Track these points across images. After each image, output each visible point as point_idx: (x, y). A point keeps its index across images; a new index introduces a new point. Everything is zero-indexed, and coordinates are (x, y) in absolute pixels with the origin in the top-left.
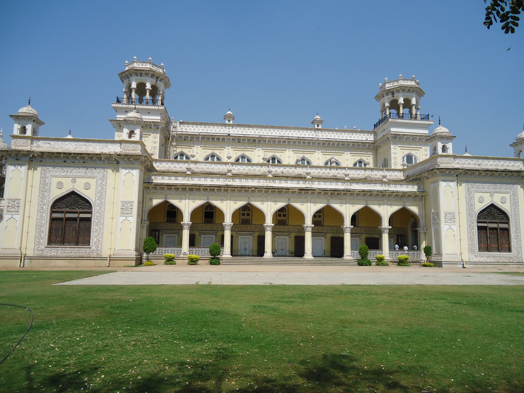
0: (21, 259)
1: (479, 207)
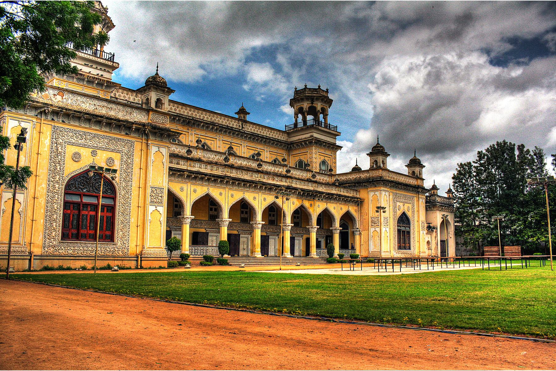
0: (30, 260)
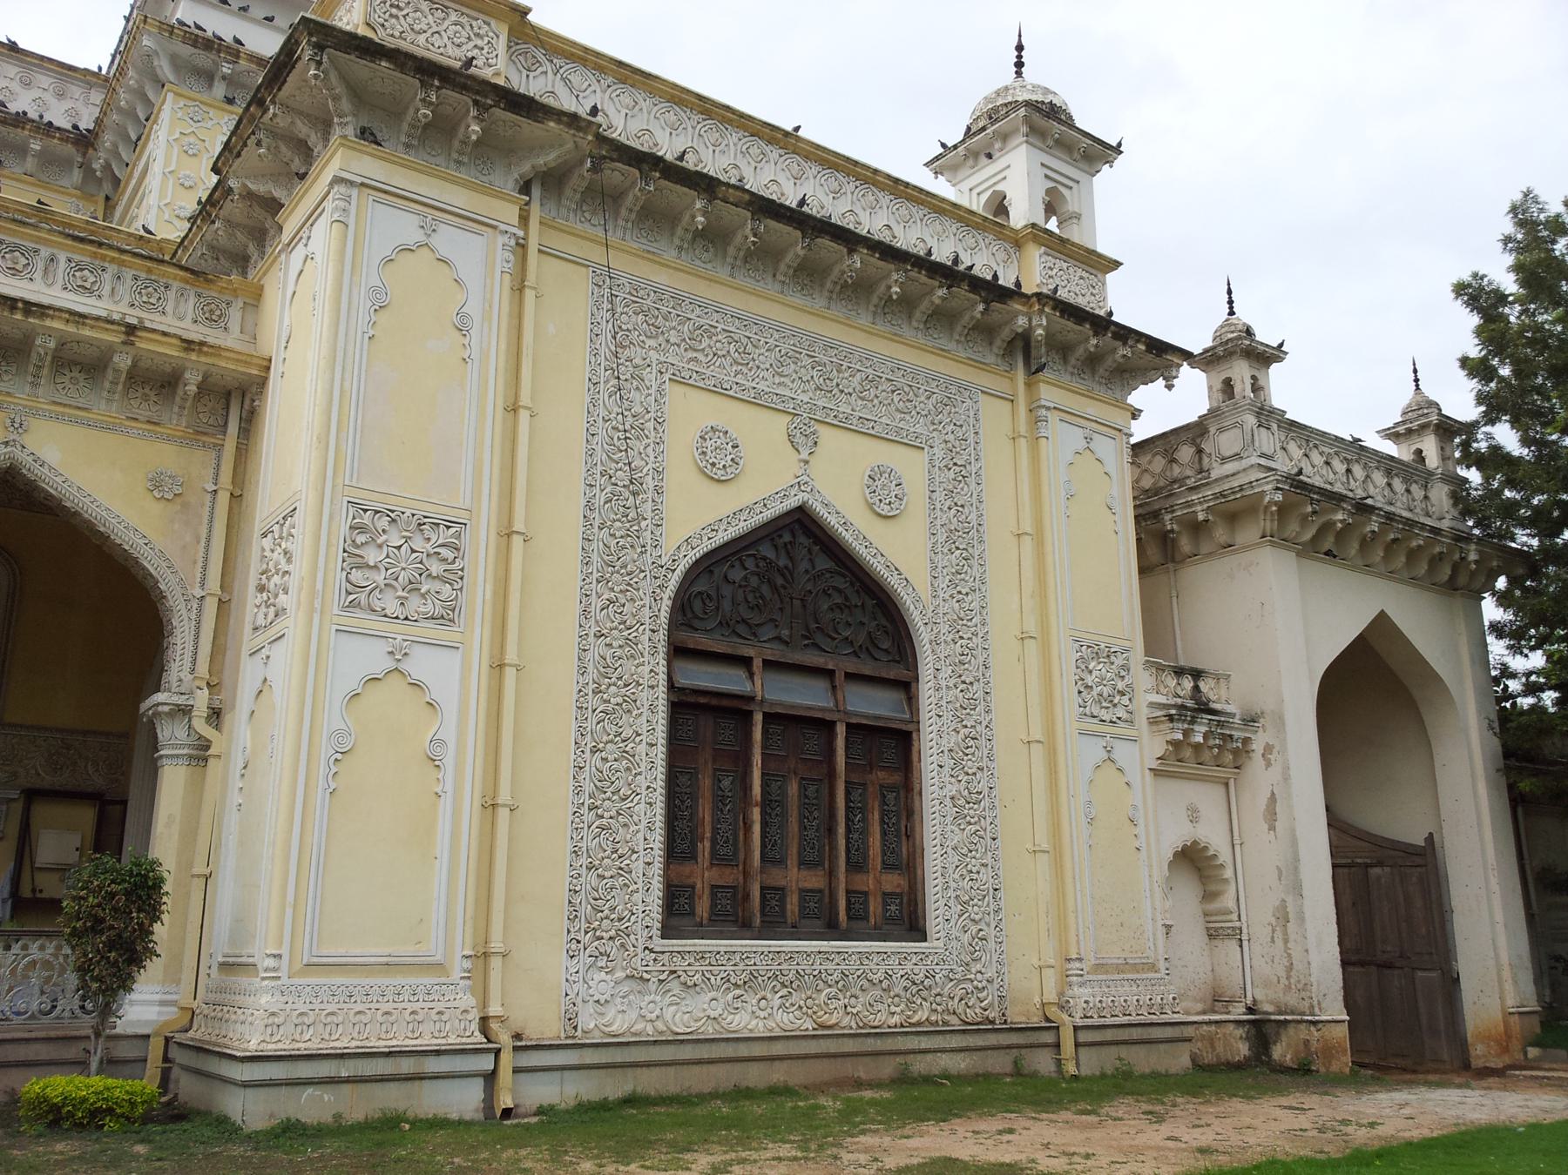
1: (699, 515)
